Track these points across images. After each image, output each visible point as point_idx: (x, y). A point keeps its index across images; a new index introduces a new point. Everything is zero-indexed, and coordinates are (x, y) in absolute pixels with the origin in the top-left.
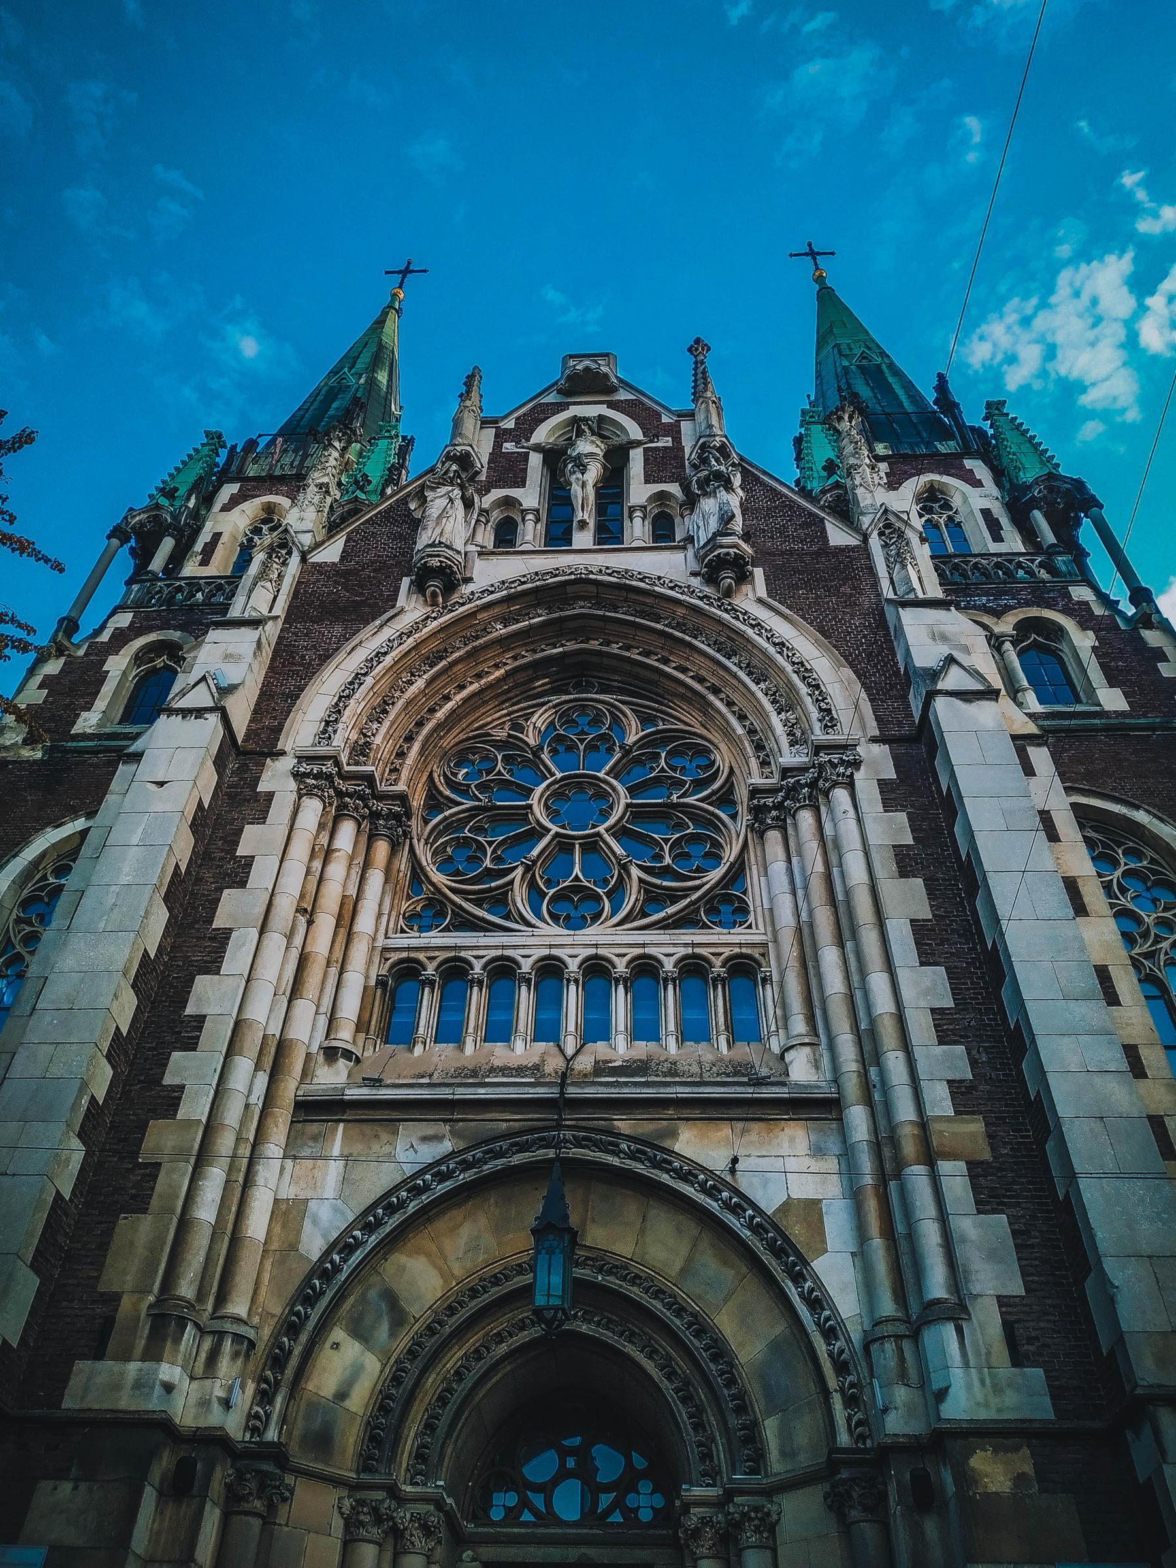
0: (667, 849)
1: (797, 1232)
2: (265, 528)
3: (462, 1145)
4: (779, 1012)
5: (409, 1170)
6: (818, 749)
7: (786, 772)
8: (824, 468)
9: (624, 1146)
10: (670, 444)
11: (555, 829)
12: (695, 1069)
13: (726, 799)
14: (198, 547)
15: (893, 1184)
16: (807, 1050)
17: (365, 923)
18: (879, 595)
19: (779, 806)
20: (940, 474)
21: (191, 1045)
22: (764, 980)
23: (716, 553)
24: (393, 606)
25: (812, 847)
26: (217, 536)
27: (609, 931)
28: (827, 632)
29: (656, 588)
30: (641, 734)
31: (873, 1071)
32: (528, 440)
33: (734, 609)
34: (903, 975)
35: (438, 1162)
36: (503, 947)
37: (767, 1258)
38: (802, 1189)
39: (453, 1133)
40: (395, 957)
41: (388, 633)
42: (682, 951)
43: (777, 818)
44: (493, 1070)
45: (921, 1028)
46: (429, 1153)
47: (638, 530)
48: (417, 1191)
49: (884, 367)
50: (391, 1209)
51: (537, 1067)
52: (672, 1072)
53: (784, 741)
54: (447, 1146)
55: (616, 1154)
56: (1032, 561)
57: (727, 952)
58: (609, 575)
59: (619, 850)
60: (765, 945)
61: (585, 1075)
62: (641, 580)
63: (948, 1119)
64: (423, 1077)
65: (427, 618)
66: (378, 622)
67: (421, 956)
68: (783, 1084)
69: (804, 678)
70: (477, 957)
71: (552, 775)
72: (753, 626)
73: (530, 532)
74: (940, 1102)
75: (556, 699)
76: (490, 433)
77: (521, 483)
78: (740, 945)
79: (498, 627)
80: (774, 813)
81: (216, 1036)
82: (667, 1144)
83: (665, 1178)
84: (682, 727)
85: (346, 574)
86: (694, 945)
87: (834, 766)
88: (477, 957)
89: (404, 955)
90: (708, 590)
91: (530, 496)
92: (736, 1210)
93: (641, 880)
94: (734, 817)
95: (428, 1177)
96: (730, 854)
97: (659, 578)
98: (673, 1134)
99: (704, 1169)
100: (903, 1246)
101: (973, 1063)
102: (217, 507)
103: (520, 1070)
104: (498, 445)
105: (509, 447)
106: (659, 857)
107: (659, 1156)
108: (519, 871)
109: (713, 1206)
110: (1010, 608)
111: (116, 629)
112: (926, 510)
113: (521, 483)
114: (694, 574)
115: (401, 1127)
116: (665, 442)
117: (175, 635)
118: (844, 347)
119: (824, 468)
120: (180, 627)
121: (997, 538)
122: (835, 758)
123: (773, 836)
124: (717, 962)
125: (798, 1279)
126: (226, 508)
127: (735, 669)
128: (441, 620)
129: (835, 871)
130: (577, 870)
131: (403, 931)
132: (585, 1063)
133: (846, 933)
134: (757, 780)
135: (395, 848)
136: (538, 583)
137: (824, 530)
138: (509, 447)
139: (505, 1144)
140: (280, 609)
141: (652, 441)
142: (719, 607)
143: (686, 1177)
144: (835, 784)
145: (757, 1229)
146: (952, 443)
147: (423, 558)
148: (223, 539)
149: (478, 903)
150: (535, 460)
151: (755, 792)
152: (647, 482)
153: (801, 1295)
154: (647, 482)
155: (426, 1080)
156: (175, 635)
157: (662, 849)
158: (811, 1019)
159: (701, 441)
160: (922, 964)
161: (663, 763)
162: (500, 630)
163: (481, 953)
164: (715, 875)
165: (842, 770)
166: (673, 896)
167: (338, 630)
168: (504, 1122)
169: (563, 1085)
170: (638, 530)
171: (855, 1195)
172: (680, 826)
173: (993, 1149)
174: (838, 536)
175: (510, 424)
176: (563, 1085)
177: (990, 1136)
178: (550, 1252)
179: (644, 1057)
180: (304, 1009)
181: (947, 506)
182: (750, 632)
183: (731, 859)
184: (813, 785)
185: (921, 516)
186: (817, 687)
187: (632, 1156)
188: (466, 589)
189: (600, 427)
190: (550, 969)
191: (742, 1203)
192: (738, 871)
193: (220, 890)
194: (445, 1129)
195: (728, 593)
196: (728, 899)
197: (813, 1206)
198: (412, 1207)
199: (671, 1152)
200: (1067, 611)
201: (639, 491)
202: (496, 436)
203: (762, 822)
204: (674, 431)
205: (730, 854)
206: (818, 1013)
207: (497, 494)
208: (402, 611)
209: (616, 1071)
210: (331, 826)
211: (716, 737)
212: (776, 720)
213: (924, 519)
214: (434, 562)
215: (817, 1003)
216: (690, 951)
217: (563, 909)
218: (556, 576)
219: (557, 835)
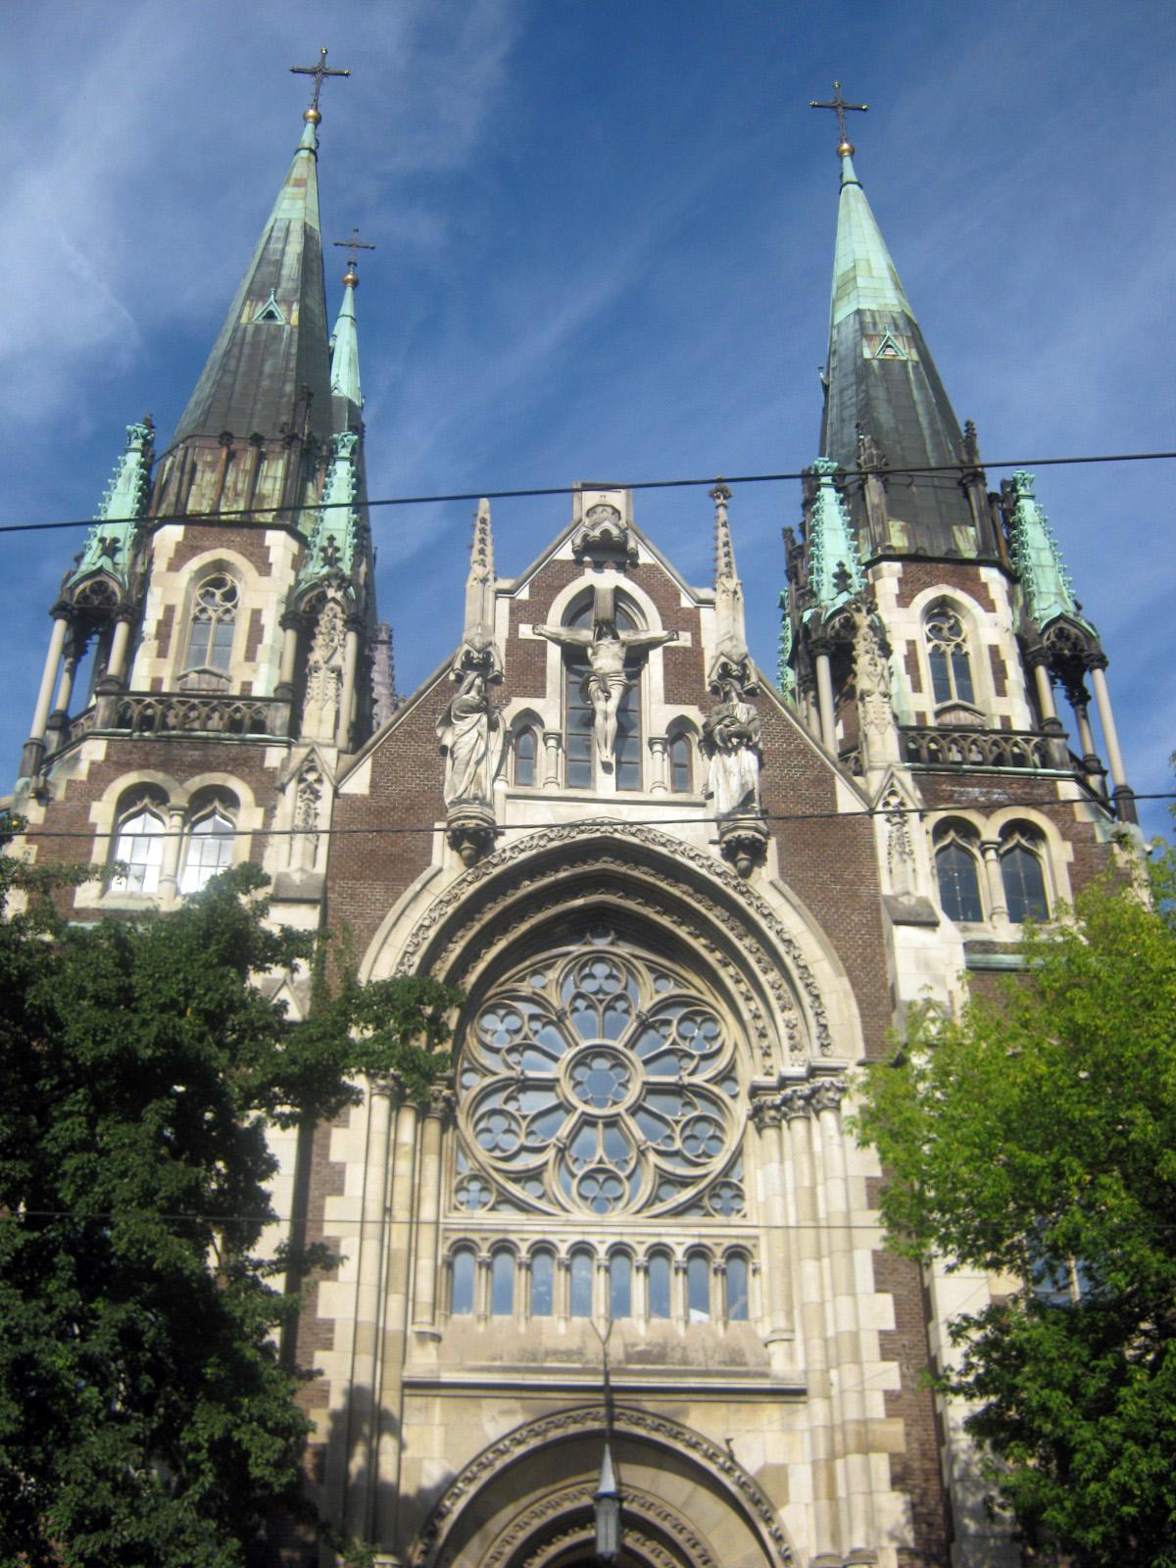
0: (678, 1129)
1: (770, 1489)
2: (218, 593)
3: (530, 1418)
4: (766, 1301)
5: (494, 1438)
6: (813, 1072)
7: (784, 1082)
8: (835, 576)
9: (649, 1422)
10: (689, 644)
11: (582, 1108)
12: (701, 1358)
13: (727, 1076)
14: (149, 626)
15: (839, 1463)
16: (785, 1344)
17: (428, 1212)
18: (877, 885)
19: (777, 1108)
20: (956, 586)
21: (328, 1345)
22: (755, 1271)
23: (736, 834)
24: (429, 864)
25: (804, 1159)
26: (169, 610)
27: (632, 1219)
28: (830, 928)
29: (678, 857)
30: (657, 998)
31: (834, 1374)
32: (544, 622)
33: (748, 891)
34: (862, 1300)
35: (514, 1431)
36: (544, 1232)
37: (748, 1506)
38: (776, 1457)
39: (525, 1409)
40: (455, 1236)
41: (427, 901)
42: (690, 1241)
43: (773, 1118)
44: (547, 1354)
45: (870, 1346)
46: (507, 1424)
47: (655, 766)
48: (503, 1453)
49: (910, 364)
50: (484, 1466)
51: (580, 1353)
52: (684, 1361)
53: (786, 1043)
54: (519, 1419)
55: (645, 1426)
56: (1027, 741)
57: (727, 1243)
58: (633, 834)
59: (639, 1134)
60: (756, 1237)
61: (620, 1362)
62: (663, 845)
63: (880, 1421)
64: (495, 1359)
65: (464, 880)
66: (416, 886)
67: (475, 1237)
68: (764, 1375)
69: (807, 985)
70: (523, 1240)
71: (577, 1044)
72: (765, 916)
73: (549, 760)
74: (877, 1408)
75: (576, 949)
76: (504, 605)
77: (539, 691)
78: (737, 1237)
79: (527, 883)
80: (773, 1113)
81: (343, 1336)
82: (680, 1420)
83: (680, 1447)
84: (693, 992)
85: (379, 813)
86: (700, 1236)
87: (828, 1090)
88: (523, 1240)
89: (461, 1235)
90: (727, 866)
91: (551, 710)
92: (728, 1471)
93: (656, 1166)
94: (734, 1097)
95: (507, 1442)
96: (731, 1142)
97: (681, 844)
98: (685, 1413)
99: (706, 1440)
100: (843, 1505)
101: (903, 1376)
102: (160, 565)
103: (568, 1354)
104: (514, 629)
105: (526, 631)
106: (670, 1137)
107: (676, 1429)
108: (550, 1155)
109: (713, 1468)
110: (1001, 805)
111: (93, 763)
112: (936, 631)
113: (539, 691)
114: (713, 842)
115: (485, 1402)
116: (685, 639)
117: (157, 777)
118: (868, 319)
119: (835, 576)
120: (164, 766)
121: (1001, 691)
122: (826, 1080)
123: (770, 1134)
124: (719, 1251)
125: (768, 1520)
126: (174, 566)
127: (745, 953)
128: (477, 885)
129: (820, 1190)
130: (600, 1152)
131: (456, 1208)
132: (616, 1350)
133: (825, 1251)
134: (761, 1079)
135: (444, 1129)
136: (567, 841)
137: (834, 793)
138: (526, 631)
139: (562, 1417)
140: (321, 868)
141: (672, 640)
142: (735, 888)
143: (694, 1446)
144: (825, 1108)
145: (743, 1485)
146: (971, 531)
147: (459, 819)
148: (178, 616)
149: (516, 1181)
150: (554, 653)
151: (755, 1091)
152: (668, 700)
153: (770, 1533)
154: (668, 700)
155: (497, 1363)
156: (157, 777)
157: (673, 1130)
158: (789, 1314)
159: (723, 659)
160: (879, 1290)
161: (675, 1035)
162: (528, 887)
163: (525, 1236)
164: (717, 1164)
165: (831, 1094)
166: (684, 1182)
167: (379, 893)
168: (561, 1401)
169: (607, 1374)
170: (655, 766)
171: (814, 1463)
172: (689, 1104)
173: (908, 1444)
174: (847, 802)
175: (524, 594)
176: (607, 1374)
177: (908, 1435)
178: (607, 1513)
179: (661, 1341)
180: (395, 1302)
181: (956, 630)
182: (763, 924)
183: (733, 1148)
184: (808, 1099)
185: (929, 640)
186: (817, 997)
187: (657, 1429)
188: (500, 843)
189: (616, 617)
190: (582, 1250)
191: (732, 1465)
192: (739, 1153)
193: (323, 1197)
194: (515, 1404)
195: (745, 873)
196: (728, 1185)
197: (780, 1473)
198: (499, 1465)
199: (684, 1426)
200: (1053, 816)
201: (657, 715)
202: (512, 612)
203: (761, 1120)
204: (692, 623)
205: (731, 1142)
206: (796, 1313)
207: (518, 704)
208: (440, 871)
209: (643, 1357)
210: (393, 1121)
211: (723, 1008)
212: (779, 1017)
213: (931, 644)
214: (471, 824)
215: (796, 1304)
216: (696, 1241)
217: (591, 1189)
218: (583, 832)
219: (583, 1113)
